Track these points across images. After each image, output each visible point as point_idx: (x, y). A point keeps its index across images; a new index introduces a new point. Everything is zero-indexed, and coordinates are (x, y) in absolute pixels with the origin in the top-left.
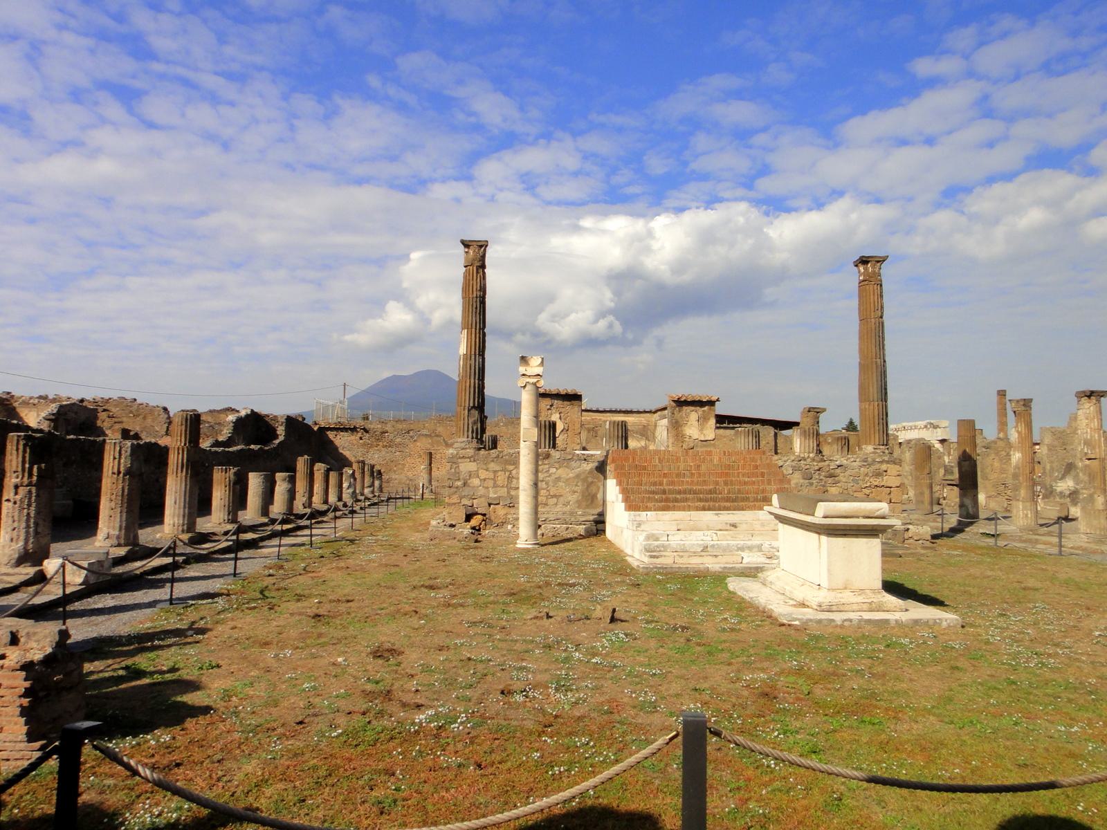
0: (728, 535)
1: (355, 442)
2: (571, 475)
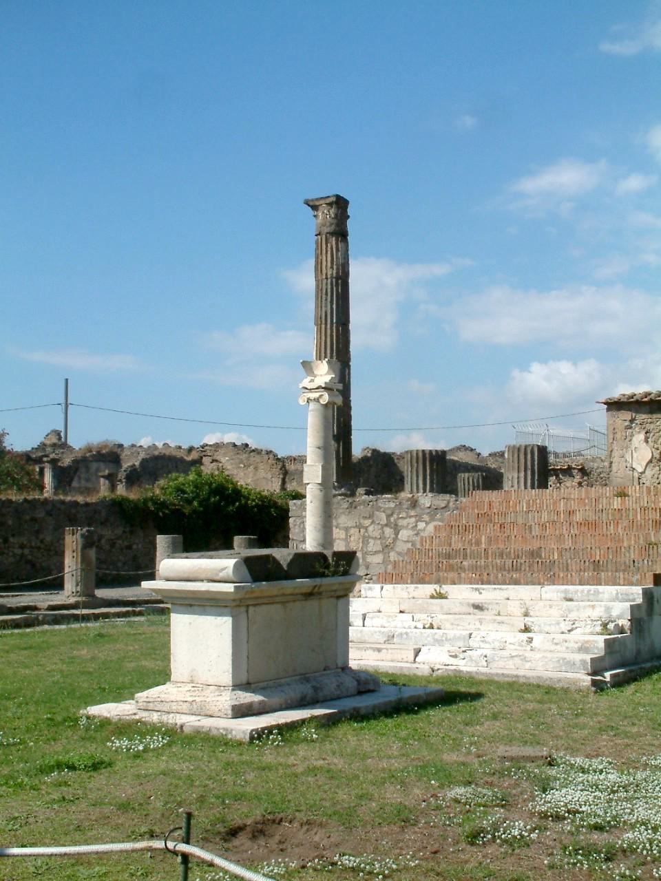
0: (447, 620)
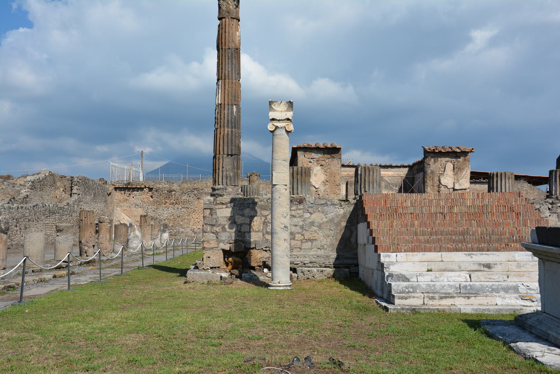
1: (146, 200)
2: (325, 220)
